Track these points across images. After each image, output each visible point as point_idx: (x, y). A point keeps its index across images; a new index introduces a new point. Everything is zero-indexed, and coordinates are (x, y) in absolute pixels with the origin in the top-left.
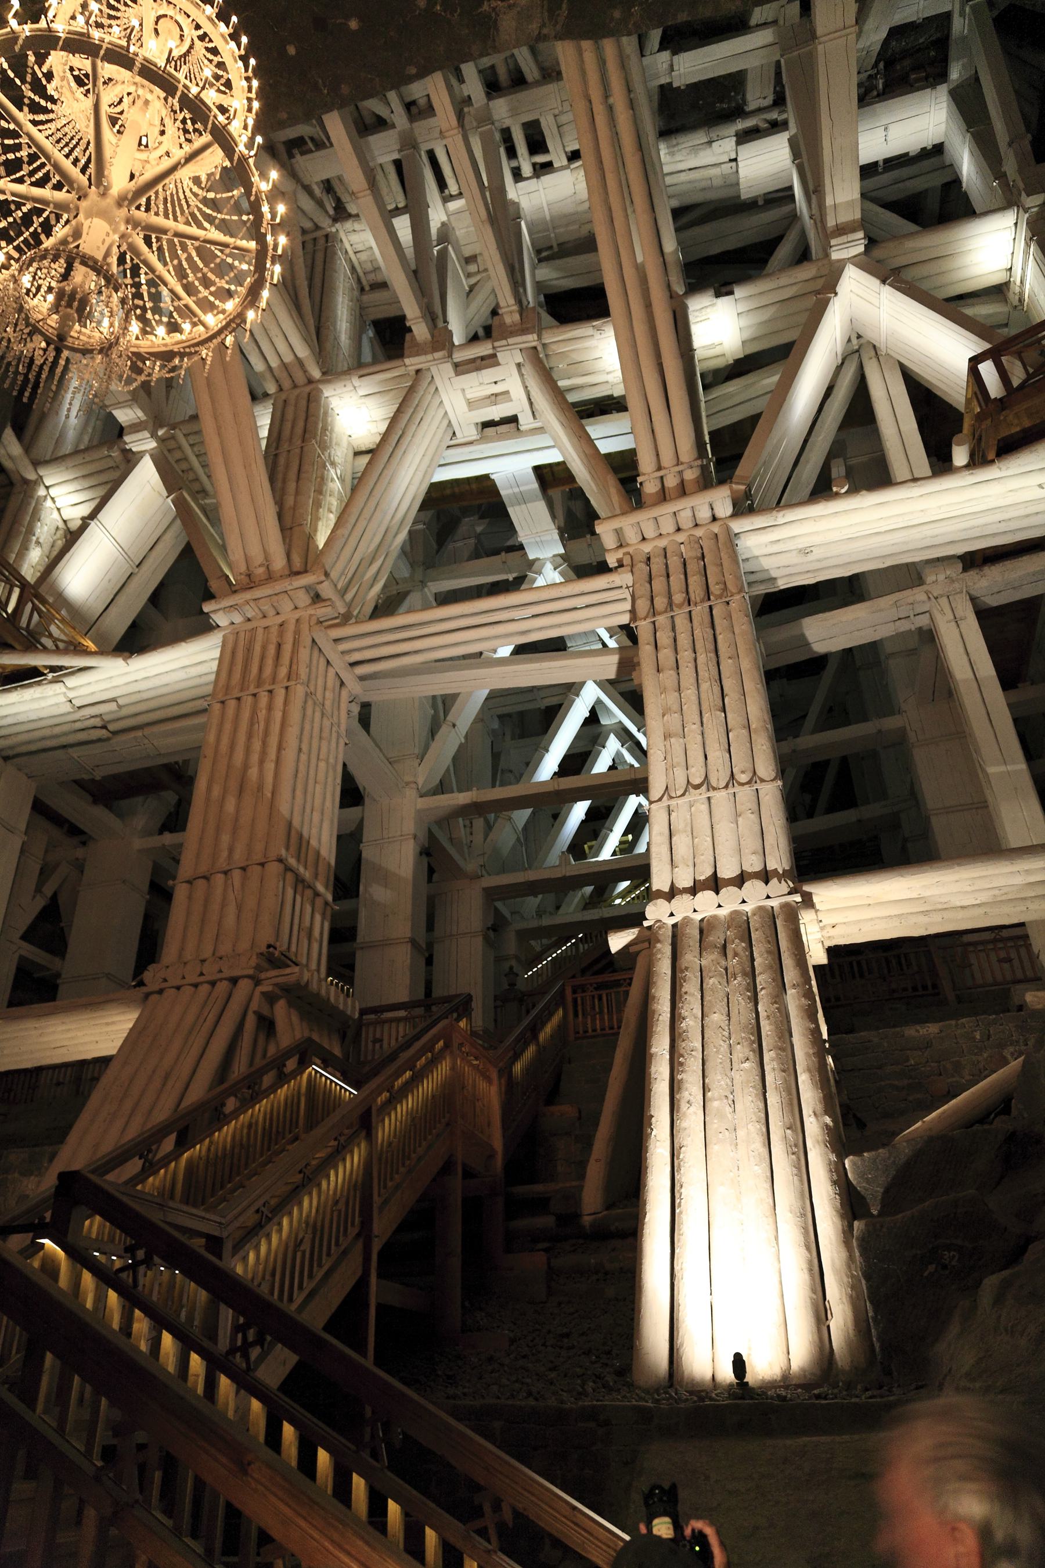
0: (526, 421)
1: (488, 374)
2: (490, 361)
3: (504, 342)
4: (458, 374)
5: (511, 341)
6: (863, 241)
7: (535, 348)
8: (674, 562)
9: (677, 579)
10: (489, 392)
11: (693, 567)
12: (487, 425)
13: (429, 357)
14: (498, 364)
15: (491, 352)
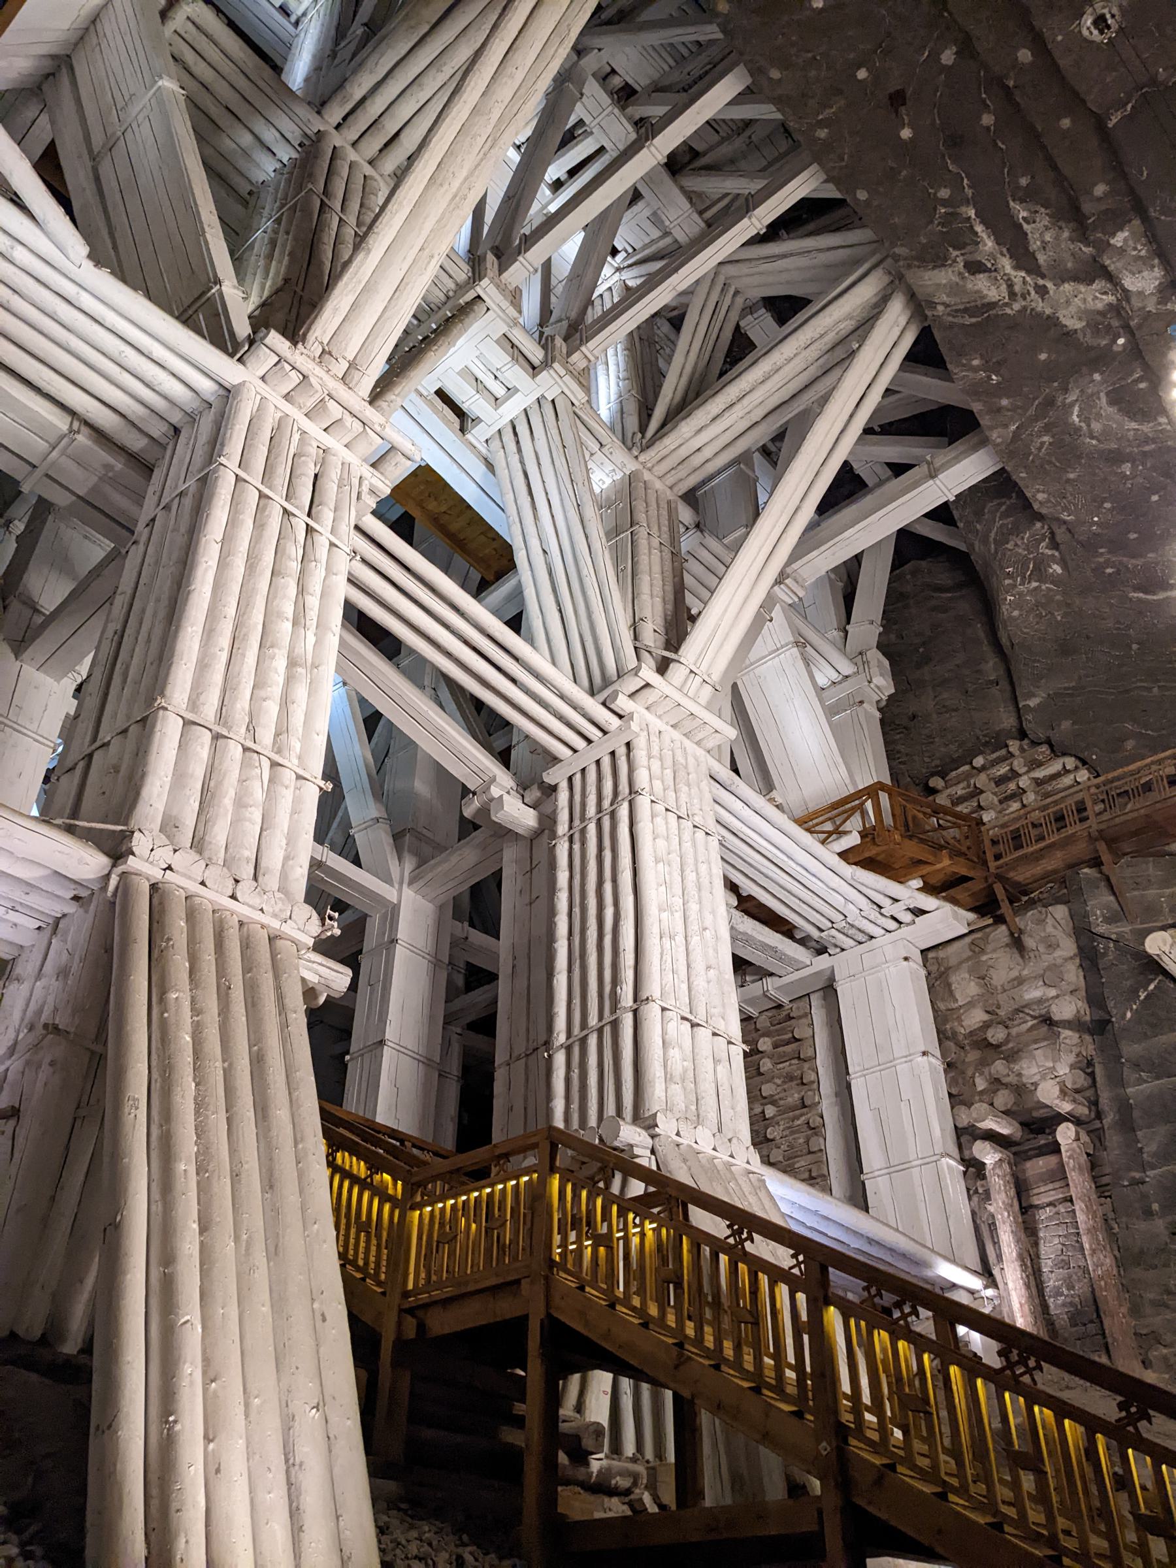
0: (477, 435)
1: (516, 375)
2: (534, 370)
3: (562, 372)
4: (497, 342)
5: (567, 378)
6: (796, 600)
7: (573, 404)
8: (668, 754)
9: (669, 773)
10: (481, 376)
11: (682, 774)
12: (441, 394)
13: (505, 304)
14: (534, 376)
15: (536, 362)
